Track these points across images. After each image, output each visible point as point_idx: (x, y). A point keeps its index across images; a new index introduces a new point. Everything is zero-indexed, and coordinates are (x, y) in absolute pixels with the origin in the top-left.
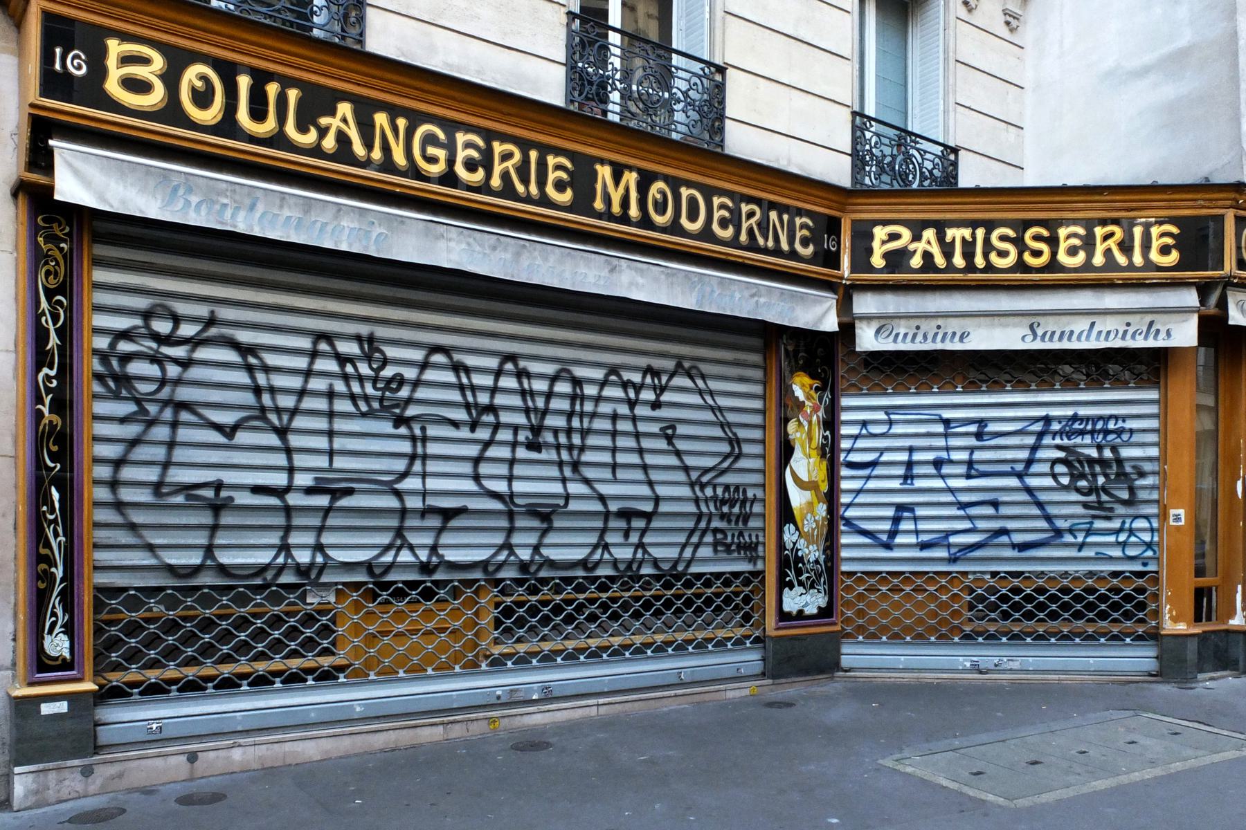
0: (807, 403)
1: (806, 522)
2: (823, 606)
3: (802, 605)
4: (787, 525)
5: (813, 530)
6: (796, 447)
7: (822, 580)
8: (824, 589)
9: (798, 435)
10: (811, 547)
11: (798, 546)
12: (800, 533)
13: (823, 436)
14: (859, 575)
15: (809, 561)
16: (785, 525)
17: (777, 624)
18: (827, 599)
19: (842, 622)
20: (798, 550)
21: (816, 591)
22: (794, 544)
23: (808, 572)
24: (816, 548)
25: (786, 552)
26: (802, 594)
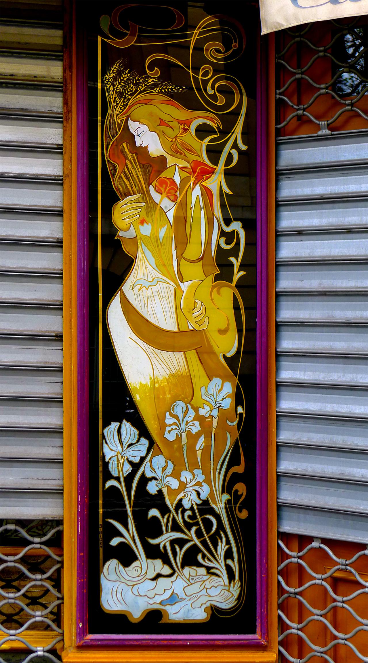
0: (171, 160)
1: (169, 420)
2: (226, 605)
3: (158, 599)
4: (115, 425)
5: (193, 438)
6: (140, 255)
7: (222, 548)
8: (229, 569)
9: (146, 230)
10: (186, 476)
11: (146, 469)
12: (152, 443)
13: (223, 234)
14: (315, 544)
15: (179, 505)
16: (106, 424)
17: (81, 634)
18: (235, 589)
19: (281, 643)
20: (144, 480)
21: (202, 571)
22: (136, 466)
23: (176, 528)
24: (201, 478)
25: (110, 483)
26: (159, 576)
